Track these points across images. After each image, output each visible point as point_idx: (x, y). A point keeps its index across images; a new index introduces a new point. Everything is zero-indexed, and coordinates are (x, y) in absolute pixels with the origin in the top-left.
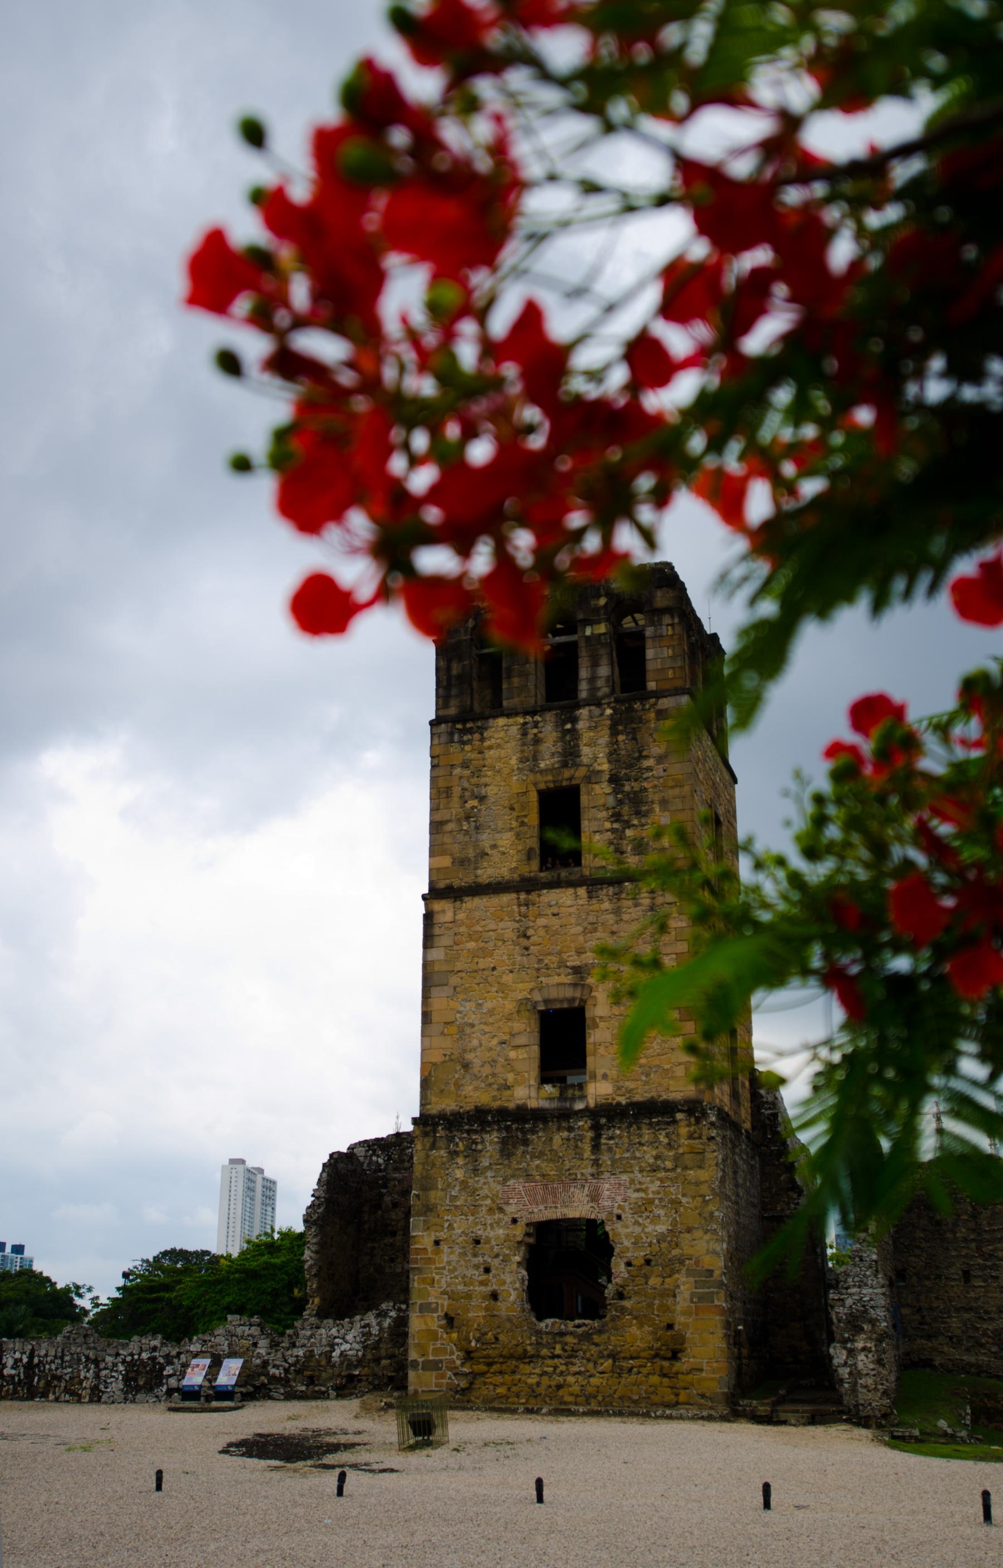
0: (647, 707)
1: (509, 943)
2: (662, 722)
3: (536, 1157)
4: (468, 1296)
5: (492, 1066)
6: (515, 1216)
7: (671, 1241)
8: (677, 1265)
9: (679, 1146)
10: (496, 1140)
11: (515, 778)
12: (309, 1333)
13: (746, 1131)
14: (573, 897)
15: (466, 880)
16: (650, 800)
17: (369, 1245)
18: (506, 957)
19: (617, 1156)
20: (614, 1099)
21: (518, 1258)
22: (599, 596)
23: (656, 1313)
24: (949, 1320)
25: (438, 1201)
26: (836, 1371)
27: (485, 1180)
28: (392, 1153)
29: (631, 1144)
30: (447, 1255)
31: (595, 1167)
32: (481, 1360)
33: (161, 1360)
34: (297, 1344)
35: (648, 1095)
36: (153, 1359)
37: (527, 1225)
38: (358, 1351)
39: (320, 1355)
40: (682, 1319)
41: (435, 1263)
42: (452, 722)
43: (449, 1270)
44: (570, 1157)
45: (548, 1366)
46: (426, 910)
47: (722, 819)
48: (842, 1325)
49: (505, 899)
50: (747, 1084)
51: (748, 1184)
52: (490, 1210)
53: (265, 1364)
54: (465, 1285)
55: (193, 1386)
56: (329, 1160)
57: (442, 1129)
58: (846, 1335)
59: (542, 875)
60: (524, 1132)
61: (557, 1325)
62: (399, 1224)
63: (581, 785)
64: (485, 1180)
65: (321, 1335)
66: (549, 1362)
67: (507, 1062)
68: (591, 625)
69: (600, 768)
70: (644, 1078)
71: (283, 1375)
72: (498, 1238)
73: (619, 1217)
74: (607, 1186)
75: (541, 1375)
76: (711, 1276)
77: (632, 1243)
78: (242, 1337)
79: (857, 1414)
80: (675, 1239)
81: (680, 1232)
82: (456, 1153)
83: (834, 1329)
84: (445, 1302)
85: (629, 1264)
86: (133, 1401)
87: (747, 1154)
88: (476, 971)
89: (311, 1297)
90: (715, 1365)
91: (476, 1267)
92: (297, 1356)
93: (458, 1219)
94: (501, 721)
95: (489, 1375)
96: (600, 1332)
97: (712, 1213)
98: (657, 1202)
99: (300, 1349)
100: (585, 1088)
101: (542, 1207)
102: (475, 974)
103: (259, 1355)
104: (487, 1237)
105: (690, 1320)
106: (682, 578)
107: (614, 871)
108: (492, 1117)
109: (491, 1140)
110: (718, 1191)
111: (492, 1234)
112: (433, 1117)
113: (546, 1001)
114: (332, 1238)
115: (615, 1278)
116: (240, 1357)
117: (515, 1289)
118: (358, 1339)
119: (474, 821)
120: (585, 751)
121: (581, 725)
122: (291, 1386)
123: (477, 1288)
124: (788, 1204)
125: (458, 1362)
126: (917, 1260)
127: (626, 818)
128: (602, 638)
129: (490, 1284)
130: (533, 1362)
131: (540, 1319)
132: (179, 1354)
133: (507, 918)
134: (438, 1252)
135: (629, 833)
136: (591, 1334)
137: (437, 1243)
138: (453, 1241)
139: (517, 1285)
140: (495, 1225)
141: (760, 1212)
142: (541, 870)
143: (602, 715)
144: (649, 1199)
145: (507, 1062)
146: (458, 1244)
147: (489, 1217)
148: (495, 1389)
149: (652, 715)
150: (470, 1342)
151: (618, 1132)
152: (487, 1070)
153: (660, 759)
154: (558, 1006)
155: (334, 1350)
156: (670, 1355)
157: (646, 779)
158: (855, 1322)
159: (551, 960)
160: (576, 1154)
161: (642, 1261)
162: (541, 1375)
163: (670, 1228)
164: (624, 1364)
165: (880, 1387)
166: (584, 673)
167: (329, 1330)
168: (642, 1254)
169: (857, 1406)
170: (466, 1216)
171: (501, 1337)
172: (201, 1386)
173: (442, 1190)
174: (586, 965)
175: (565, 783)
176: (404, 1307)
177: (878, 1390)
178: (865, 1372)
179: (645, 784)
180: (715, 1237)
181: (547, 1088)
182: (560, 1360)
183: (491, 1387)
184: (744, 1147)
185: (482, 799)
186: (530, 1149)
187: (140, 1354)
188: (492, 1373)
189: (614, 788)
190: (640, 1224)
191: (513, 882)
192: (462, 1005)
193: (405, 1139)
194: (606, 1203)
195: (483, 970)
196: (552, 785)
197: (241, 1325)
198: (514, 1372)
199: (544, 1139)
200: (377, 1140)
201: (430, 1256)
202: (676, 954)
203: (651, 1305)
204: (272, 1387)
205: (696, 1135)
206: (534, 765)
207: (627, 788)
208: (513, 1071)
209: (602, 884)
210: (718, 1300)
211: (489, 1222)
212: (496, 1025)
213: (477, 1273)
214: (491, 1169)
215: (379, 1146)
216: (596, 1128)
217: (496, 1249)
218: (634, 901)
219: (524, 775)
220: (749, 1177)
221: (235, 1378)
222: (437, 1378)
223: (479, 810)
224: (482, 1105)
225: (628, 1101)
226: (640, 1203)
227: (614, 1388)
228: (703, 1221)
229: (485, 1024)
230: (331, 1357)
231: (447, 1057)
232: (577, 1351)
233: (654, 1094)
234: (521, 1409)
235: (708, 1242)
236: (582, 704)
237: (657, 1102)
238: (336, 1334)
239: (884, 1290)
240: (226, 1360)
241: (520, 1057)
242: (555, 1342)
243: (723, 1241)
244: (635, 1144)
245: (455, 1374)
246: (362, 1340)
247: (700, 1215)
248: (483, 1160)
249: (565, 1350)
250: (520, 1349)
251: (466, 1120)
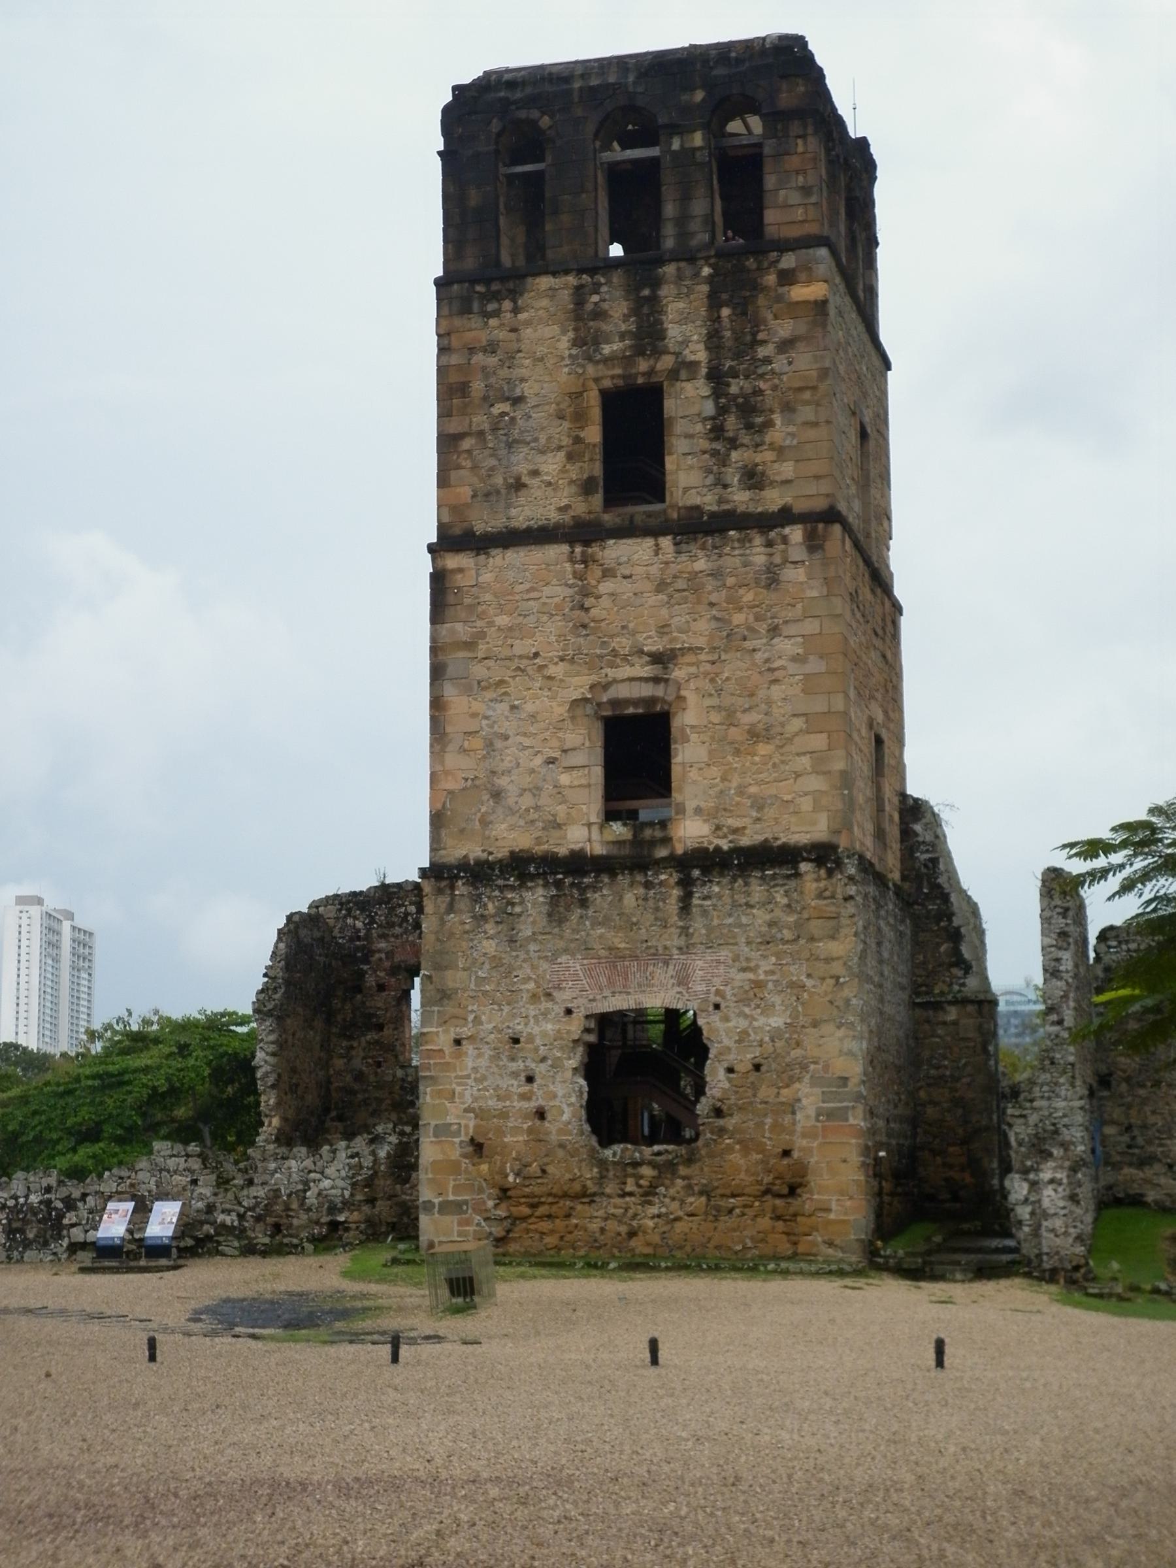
0: (766, 265)
1: (559, 618)
2: (786, 288)
3: (600, 924)
4: (504, 1115)
5: (534, 795)
7: (790, 1039)
8: (797, 1071)
9: (804, 908)
10: (541, 899)
11: (566, 370)
12: (272, 1166)
13: (895, 885)
14: (650, 552)
15: (493, 523)
16: (768, 406)
17: (344, 1044)
18: (554, 639)
19: (716, 922)
20: (710, 843)
21: (573, 1063)
22: (692, 89)
23: (767, 1135)
24: (1168, 1142)
25: (458, 985)
26: (1013, 1210)
28: (376, 913)
29: (735, 905)
30: (471, 1058)
31: (683, 938)
32: (523, 1200)
33: (60, 1205)
34: (256, 1181)
35: (759, 838)
36: (48, 1203)
37: (587, 1017)
38: (343, 1189)
39: (289, 1196)
40: (804, 1143)
41: (455, 1071)
42: (469, 281)
43: (475, 1079)
44: (648, 924)
45: (615, 1207)
46: (433, 567)
47: (869, 430)
48: (1023, 1149)
49: (552, 552)
50: (896, 817)
51: (895, 958)
52: (534, 998)
53: (210, 1208)
54: (498, 1100)
55: (113, 1238)
56: (287, 925)
57: (464, 884)
58: (1029, 1163)
59: (608, 518)
60: (583, 890)
61: (628, 1154)
62: (388, 1015)
63: (665, 384)
65: (290, 1168)
66: (618, 1201)
67: (556, 790)
68: (681, 134)
69: (693, 358)
70: (754, 814)
71: (236, 1223)
72: (544, 1034)
75: (606, 1219)
76: (845, 1085)
77: (736, 1042)
78: (175, 1172)
79: (1040, 1265)
80: (795, 1036)
81: (803, 1026)
83: (1013, 1154)
84: (471, 1123)
85: (730, 1070)
86: (21, 1261)
87: (895, 917)
88: (509, 659)
89: (266, 1116)
90: (848, 1203)
91: (515, 1075)
92: (255, 1197)
93: (487, 1009)
94: (545, 282)
95: (532, 1220)
96: (689, 1161)
97: (847, 1001)
99: (260, 1188)
100: (669, 826)
101: (607, 993)
102: (507, 663)
103: (201, 1197)
104: (530, 1034)
105: (815, 1145)
106: (820, 60)
107: (713, 515)
108: (536, 868)
109: (536, 897)
110: (856, 970)
111: (536, 1030)
112: (450, 868)
113: (615, 703)
114: (294, 1035)
115: (711, 1089)
116: (174, 1200)
117: (569, 1105)
118: (343, 1173)
119: (505, 435)
120: (674, 332)
121: (666, 291)
122: (248, 1238)
123: (515, 1104)
124: (951, 985)
125: (490, 1204)
126: (1128, 1061)
127: (731, 434)
128: (698, 154)
129: (534, 1098)
130: (594, 1201)
131: (605, 1142)
132: (84, 1196)
133: (555, 581)
134: (459, 1056)
135: (735, 455)
136: (677, 1164)
137: (458, 1042)
139: (573, 1099)
141: (910, 997)
142: (604, 512)
143: (697, 274)
144: (761, 981)
145: (556, 790)
146: (487, 1043)
147: (532, 1007)
148: (541, 1239)
149: (771, 279)
150: (507, 1176)
151: (716, 889)
152: (527, 801)
153: (786, 346)
154: (631, 710)
155: (309, 1189)
156: (785, 1191)
157: (762, 376)
158: (1040, 1148)
159: (623, 644)
160: (656, 919)
161: (750, 1067)
162: (606, 1219)
163: (789, 1021)
164: (722, 1203)
165: (1072, 1230)
166: (670, 209)
167: (298, 1162)
168: (749, 1056)
169: (1039, 1256)
171: (550, 1169)
172: (123, 1239)
173: (464, 969)
174: (672, 650)
175: (640, 381)
176: (408, 1129)
177: (1069, 1235)
178: (1052, 1211)
179: (762, 385)
180: (851, 1033)
181: (615, 827)
182: (633, 1199)
183: (537, 1236)
184: (891, 907)
185: (518, 401)
186: (590, 912)
187: (27, 1197)
188: (540, 1217)
189: (713, 388)
190: (746, 1016)
191: (564, 527)
192: (489, 708)
193: (395, 893)
194: (699, 988)
195: (521, 657)
196: (620, 382)
197: (174, 1156)
198: (568, 1216)
199: (610, 898)
200: (354, 894)
201: (448, 1059)
202: (803, 636)
203: (759, 1125)
204: (221, 1239)
205: (827, 894)
206: (595, 351)
207: (734, 389)
208: (564, 802)
209: (695, 533)
210: (855, 1118)
211: (532, 1013)
212: (542, 736)
213: (516, 1083)
214: (535, 940)
215: (356, 904)
216: (686, 884)
217: (543, 1051)
218: (743, 558)
219: (579, 365)
220: (896, 948)
221: (173, 1226)
222: (460, 1224)
223: (513, 419)
224: (521, 851)
225: (731, 845)
226: (747, 988)
227: (708, 1235)
228: (835, 1012)
229: (525, 734)
230: (305, 1198)
231: (470, 782)
232: (656, 1187)
233: (769, 835)
234: (580, 1265)
235: (841, 1040)
236: (667, 256)
237: (772, 848)
238: (312, 1167)
239: (1082, 1102)
240: (157, 1203)
241: (576, 783)
242: (626, 1176)
243: (862, 1038)
244: (740, 906)
245: (486, 1219)
246: (350, 1174)
247: (831, 1002)
248: (522, 927)
249: (640, 1186)
250: (577, 1187)
251: (497, 872)
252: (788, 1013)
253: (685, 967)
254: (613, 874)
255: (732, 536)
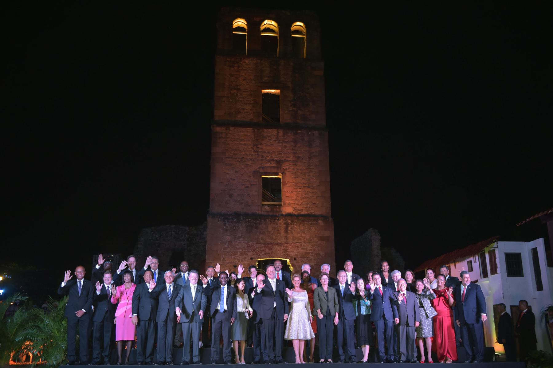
6: (252, 257)
27: (239, 242)
64: (239, 242)
73: (295, 259)
74: (291, 246)
82: (227, 230)
98: (311, 254)
135: (300, 112)
138: (225, 265)
140: (243, 260)
146: (227, 266)
151: (295, 226)
163: (316, 264)
170: (231, 255)
181: (265, 207)
185: (239, 90)
186: (259, 230)
195: (238, 158)
211: (241, 258)
216: (287, 225)
226: (304, 254)
251: (231, 218)
252: (315, 262)
253: (287, 247)
254: (265, 220)
255: (299, 133)
